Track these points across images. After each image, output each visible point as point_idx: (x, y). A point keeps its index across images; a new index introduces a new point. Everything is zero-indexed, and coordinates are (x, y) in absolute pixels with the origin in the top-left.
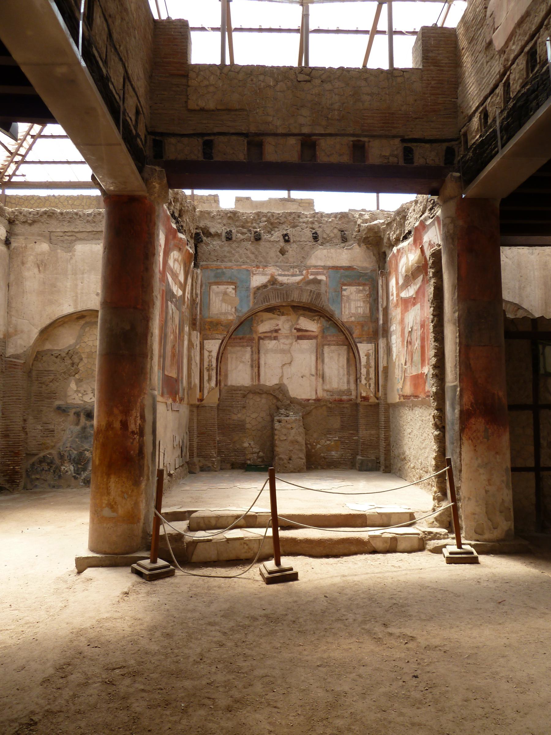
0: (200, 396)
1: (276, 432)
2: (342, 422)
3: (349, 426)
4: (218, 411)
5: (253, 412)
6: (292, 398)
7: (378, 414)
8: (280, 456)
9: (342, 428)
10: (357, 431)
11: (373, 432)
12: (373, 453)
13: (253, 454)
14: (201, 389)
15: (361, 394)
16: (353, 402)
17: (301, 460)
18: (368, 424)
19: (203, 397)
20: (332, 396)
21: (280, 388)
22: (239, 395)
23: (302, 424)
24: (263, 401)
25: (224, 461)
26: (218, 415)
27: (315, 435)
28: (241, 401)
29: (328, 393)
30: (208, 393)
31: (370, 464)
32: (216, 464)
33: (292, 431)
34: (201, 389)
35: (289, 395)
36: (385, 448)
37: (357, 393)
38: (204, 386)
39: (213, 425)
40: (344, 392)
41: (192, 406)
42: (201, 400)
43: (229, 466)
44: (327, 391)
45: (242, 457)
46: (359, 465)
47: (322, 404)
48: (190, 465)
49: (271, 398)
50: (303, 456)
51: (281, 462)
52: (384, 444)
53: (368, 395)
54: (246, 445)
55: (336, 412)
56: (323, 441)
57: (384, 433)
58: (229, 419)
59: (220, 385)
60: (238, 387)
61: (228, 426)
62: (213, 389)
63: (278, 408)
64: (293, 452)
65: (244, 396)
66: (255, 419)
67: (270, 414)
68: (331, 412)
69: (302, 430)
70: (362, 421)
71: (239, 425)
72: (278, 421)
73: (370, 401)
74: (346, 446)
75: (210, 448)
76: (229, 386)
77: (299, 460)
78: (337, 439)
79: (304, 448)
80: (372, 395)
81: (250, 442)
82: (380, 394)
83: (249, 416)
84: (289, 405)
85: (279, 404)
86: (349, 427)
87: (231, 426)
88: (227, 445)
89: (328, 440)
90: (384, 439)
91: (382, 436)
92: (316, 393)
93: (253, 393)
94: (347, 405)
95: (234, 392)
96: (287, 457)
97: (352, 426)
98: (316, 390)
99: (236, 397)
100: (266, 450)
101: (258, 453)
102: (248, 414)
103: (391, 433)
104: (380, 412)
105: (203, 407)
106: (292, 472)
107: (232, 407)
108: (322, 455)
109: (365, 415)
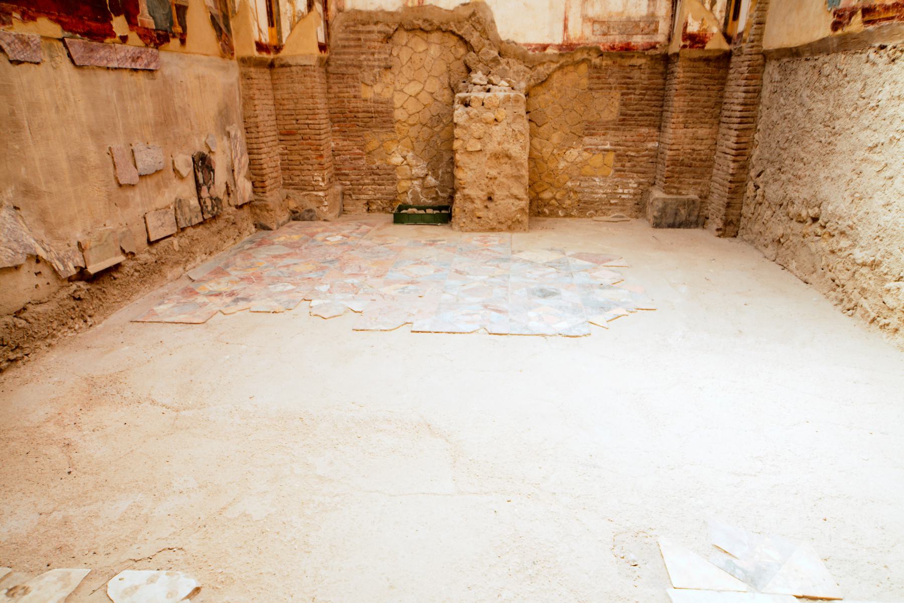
0: (272, 37)
1: (457, 132)
2: (624, 105)
3: (640, 115)
4: (328, 78)
5: (410, 81)
6: (502, 42)
7: (723, 82)
8: (466, 191)
9: (624, 120)
10: (659, 128)
11: (702, 132)
12: (695, 184)
13: (411, 179)
14: (273, 18)
15: (685, 27)
16: (658, 52)
17: (517, 202)
18: (691, 111)
19: (280, 40)
20: (605, 34)
21: (474, 14)
22: (374, 36)
23: (522, 111)
24: (432, 52)
25: (350, 195)
26: (329, 88)
27: (555, 138)
28: (379, 53)
29: (597, 26)
30: (292, 29)
31: (683, 212)
32: (326, 203)
33: (498, 128)
34: (273, 18)
35: (497, 35)
36: (732, 175)
37: (672, 27)
38: (279, 9)
39: (311, 112)
40: (637, 24)
41: (244, 61)
42: (275, 47)
43: (361, 206)
44: (594, 21)
45: (388, 187)
46: (655, 214)
47: (579, 56)
48: (258, 211)
49: (453, 41)
50: (520, 191)
51: (469, 206)
52: (732, 165)
53: (705, 30)
54: (397, 159)
55: (611, 80)
56: (574, 152)
57: (738, 136)
58: (355, 97)
59: (326, 9)
60: (370, 13)
61: (353, 115)
62: (302, 17)
63: (469, 70)
64: (497, 182)
65: (388, 38)
66: (415, 97)
67: (450, 85)
68: (599, 78)
69: (523, 125)
70: (678, 103)
71: (378, 112)
72: (462, 103)
73: (708, 46)
74: (628, 164)
75: (310, 167)
76: (348, 13)
77: (511, 201)
78: (608, 147)
79: (525, 172)
80: (715, 30)
81: (405, 153)
82: (741, 24)
83: (402, 91)
84: (495, 61)
85: (471, 57)
86: (640, 118)
87: (360, 115)
88: (355, 159)
89: (586, 150)
90: (734, 152)
91: (730, 141)
92: (566, 27)
93: (407, 30)
94: (642, 61)
95: (361, 28)
96: (483, 195)
97: (648, 115)
98: (566, 19)
99: (366, 40)
100: (440, 172)
101: (424, 178)
102: (398, 88)
103: (756, 136)
104: (730, 77)
105: (283, 66)
106: (493, 229)
107: (360, 67)
108: (569, 184)
109: (688, 85)
